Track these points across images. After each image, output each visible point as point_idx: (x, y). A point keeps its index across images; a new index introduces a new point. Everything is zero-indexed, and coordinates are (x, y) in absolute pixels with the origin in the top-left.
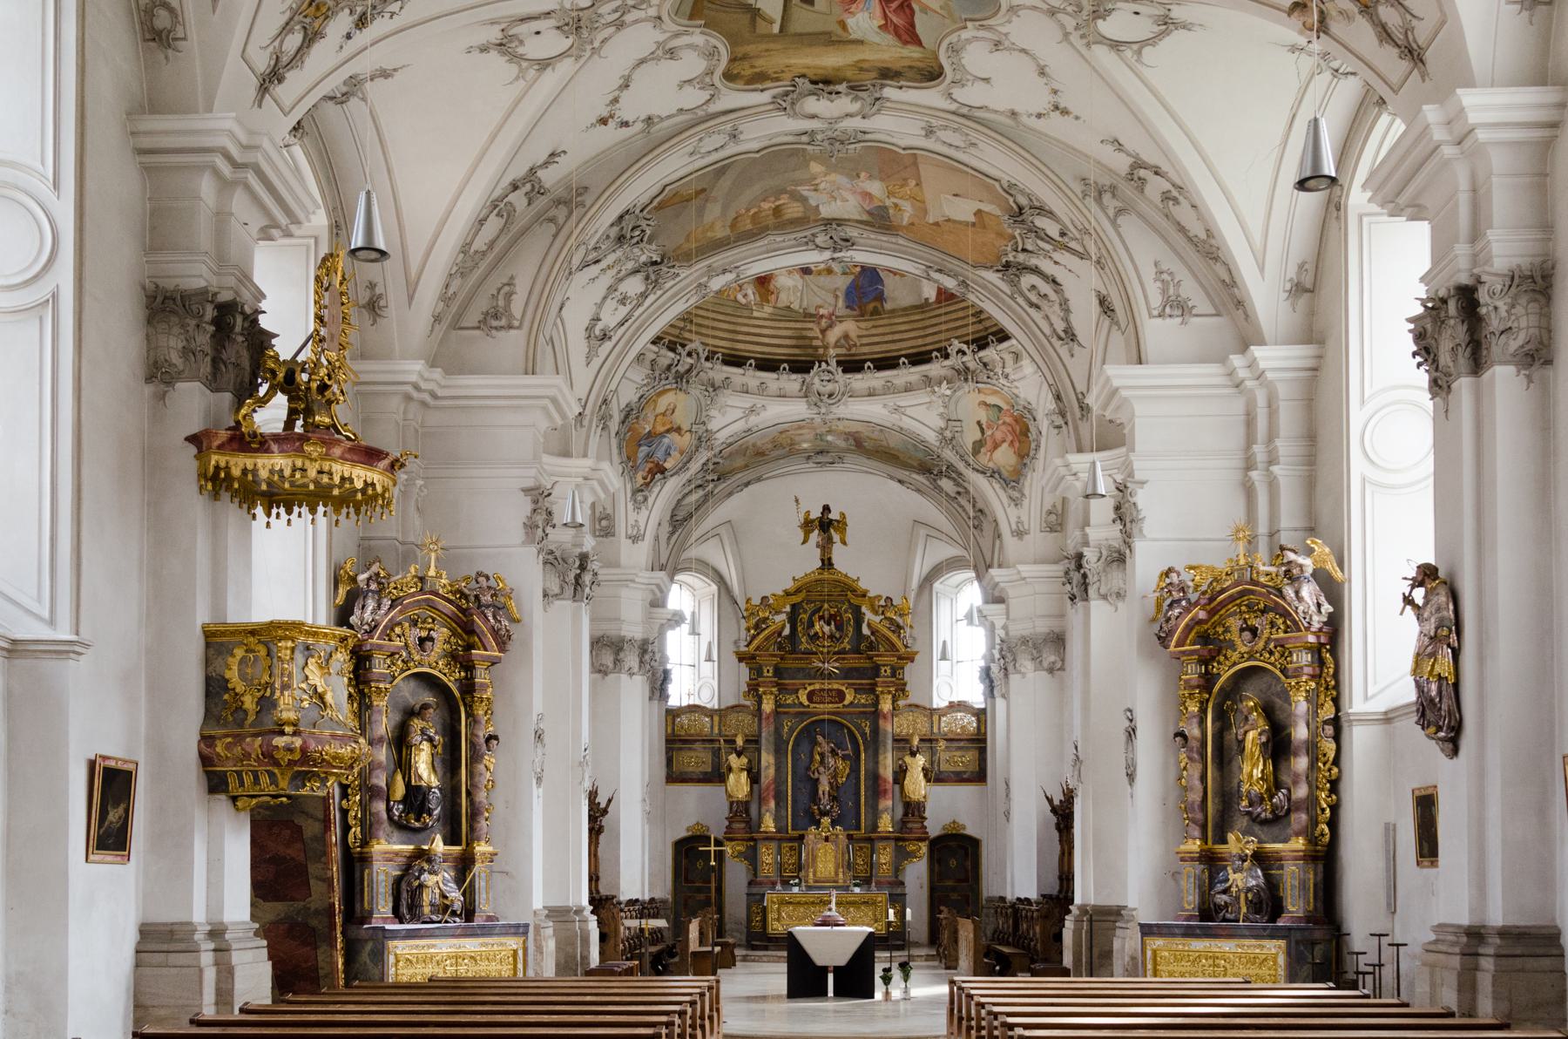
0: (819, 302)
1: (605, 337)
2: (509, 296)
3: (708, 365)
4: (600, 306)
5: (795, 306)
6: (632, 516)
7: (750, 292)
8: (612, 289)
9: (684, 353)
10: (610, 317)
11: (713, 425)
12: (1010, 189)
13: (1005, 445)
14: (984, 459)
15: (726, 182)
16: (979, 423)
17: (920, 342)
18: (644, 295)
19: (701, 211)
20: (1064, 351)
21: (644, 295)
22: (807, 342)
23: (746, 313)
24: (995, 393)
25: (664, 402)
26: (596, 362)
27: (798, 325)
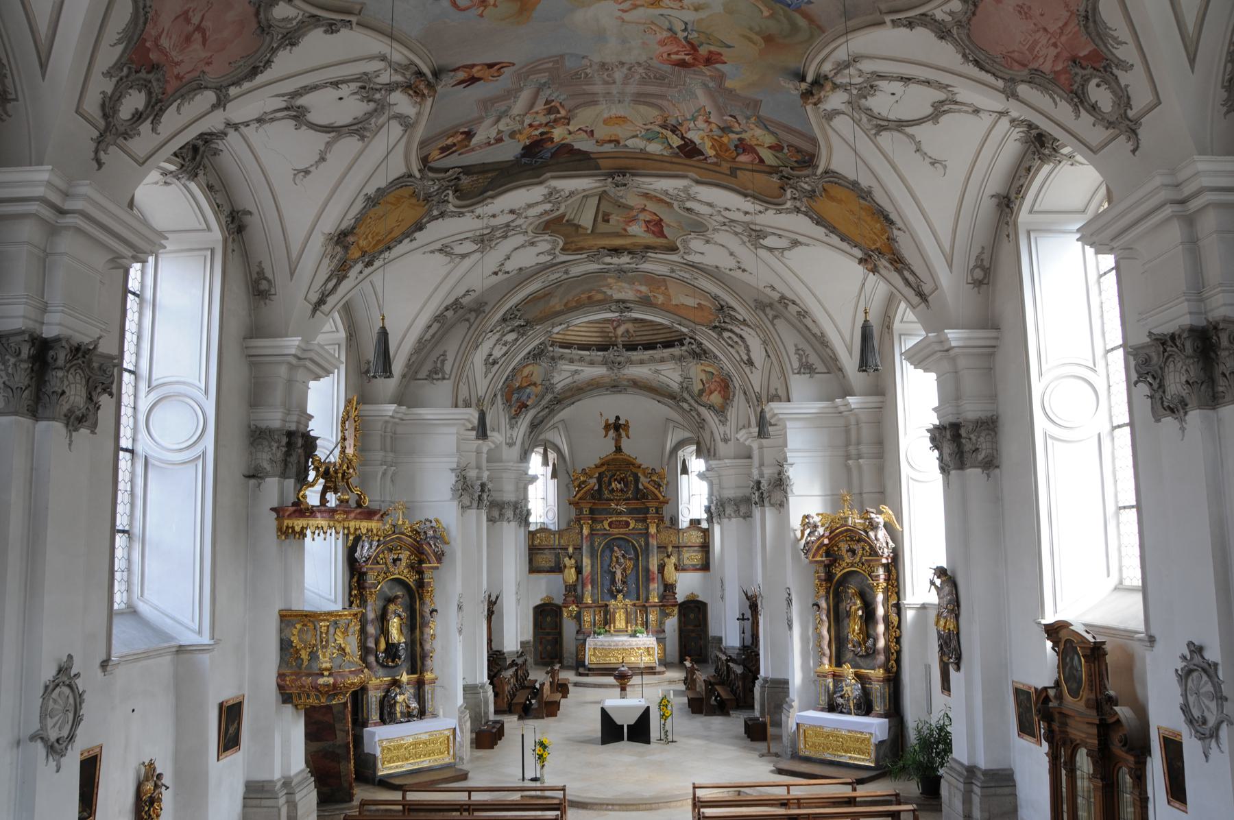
1: (494, 363)
10: (497, 353)
11: (555, 381)
12: (716, 298)
14: (704, 399)
18: (517, 340)
21: (517, 340)
26: (490, 376)
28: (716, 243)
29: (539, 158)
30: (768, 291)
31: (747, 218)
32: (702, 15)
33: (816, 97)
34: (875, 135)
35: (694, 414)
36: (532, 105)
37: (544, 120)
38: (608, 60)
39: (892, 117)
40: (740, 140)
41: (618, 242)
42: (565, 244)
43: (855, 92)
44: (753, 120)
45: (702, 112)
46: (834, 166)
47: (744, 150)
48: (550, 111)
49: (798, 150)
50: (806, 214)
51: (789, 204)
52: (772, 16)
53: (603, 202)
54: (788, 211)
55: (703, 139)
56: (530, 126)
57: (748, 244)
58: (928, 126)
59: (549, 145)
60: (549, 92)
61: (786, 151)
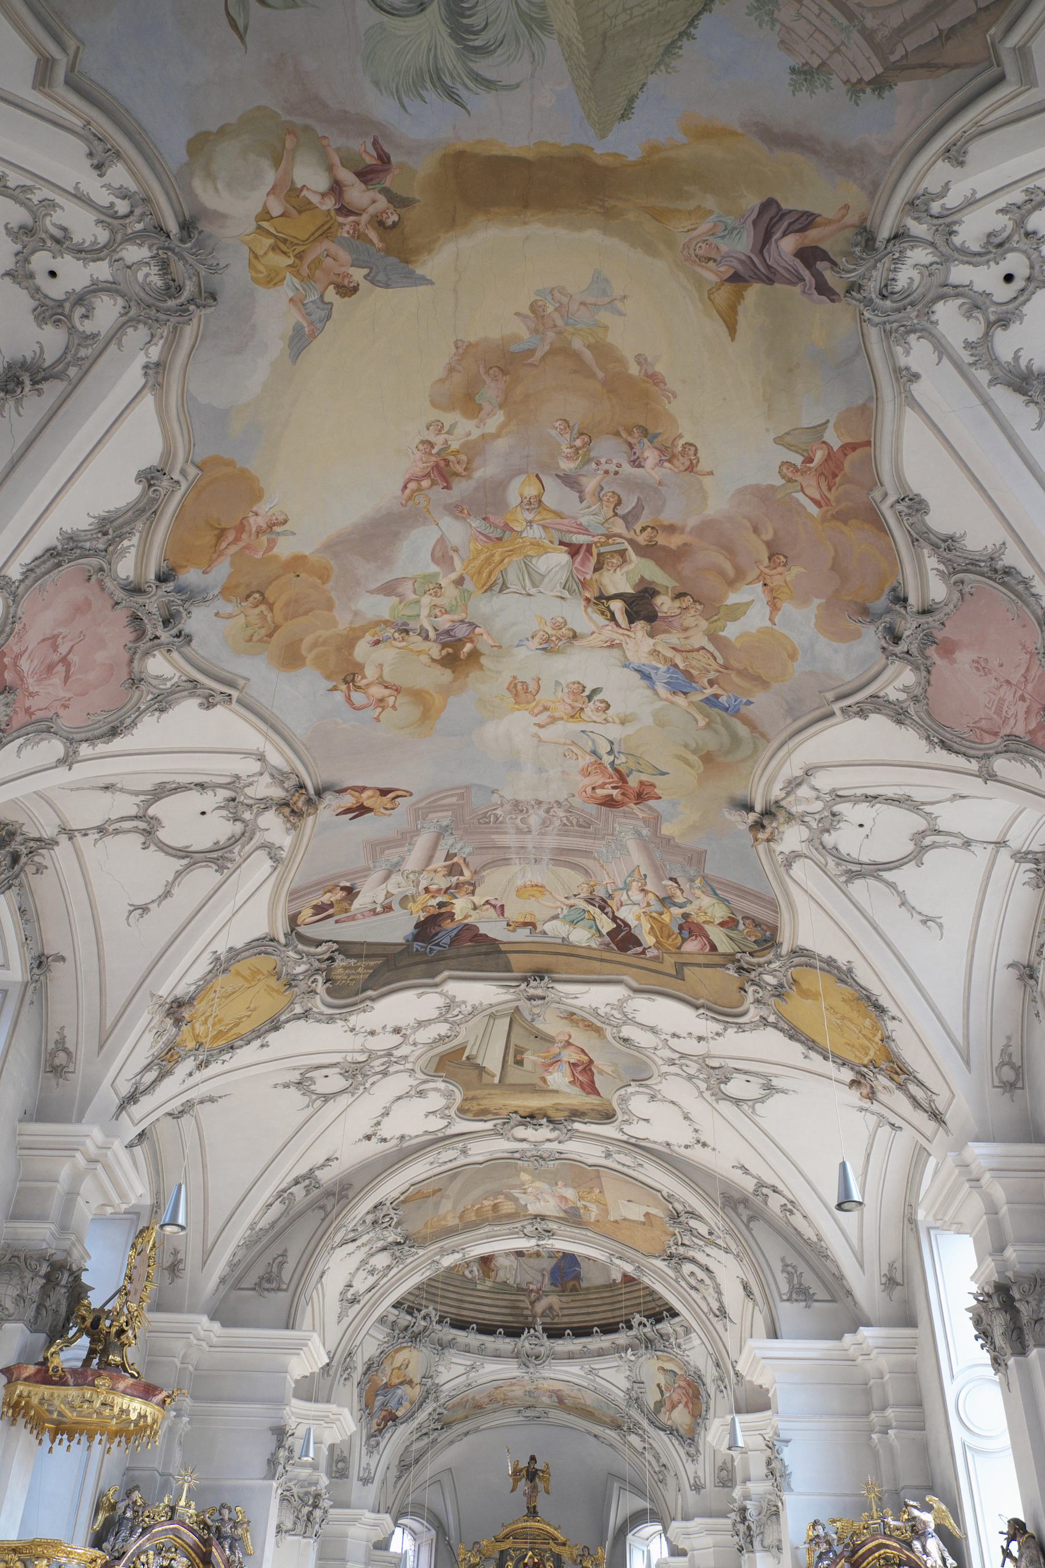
0: (530, 1279)
1: (354, 1301)
2: (282, 1263)
3: (438, 1327)
4: (352, 1275)
5: (511, 1282)
6: (365, 1459)
7: (475, 1269)
8: (365, 1262)
9: (419, 1317)
10: (361, 1284)
11: (440, 1380)
13: (681, 1406)
14: (663, 1417)
15: (457, 1185)
16: (658, 1385)
17: (609, 1315)
18: (389, 1268)
19: (437, 1205)
20: (719, 1326)
21: (389, 1268)
22: (519, 1312)
23: (471, 1286)
24: (671, 1360)
25: (400, 1358)
26: (346, 1321)
27: (513, 1297)
28: (664, 1100)
29: (438, 946)
30: (737, 1177)
31: (700, 1049)
32: (630, 730)
33: (769, 830)
34: (846, 882)
35: (648, 1456)
36: (430, 859)
37: (442, 882)
38: (521, 797)
39: (864, 859)
40: (685, 916)
41: (534, 1103)
42: (465, 1100)
43: (814, 825)
44: (698, 883)
45: (636, 876)
46: (805, 941)
47: (691, 933)
48: (453, 870)
49: (757, 924)
50: (775, 1026)
51: (754, 1014)
52: (708, 726)
53: (516, 1028)
54: (754, 1026)
55: (638, 918)
56: (427, 890)
57: (707, 1095)
58: (910, 868)
59: (448, 925)
60: (450, 840)
61: (741, 927)
